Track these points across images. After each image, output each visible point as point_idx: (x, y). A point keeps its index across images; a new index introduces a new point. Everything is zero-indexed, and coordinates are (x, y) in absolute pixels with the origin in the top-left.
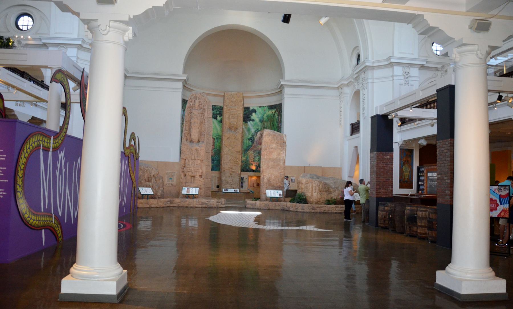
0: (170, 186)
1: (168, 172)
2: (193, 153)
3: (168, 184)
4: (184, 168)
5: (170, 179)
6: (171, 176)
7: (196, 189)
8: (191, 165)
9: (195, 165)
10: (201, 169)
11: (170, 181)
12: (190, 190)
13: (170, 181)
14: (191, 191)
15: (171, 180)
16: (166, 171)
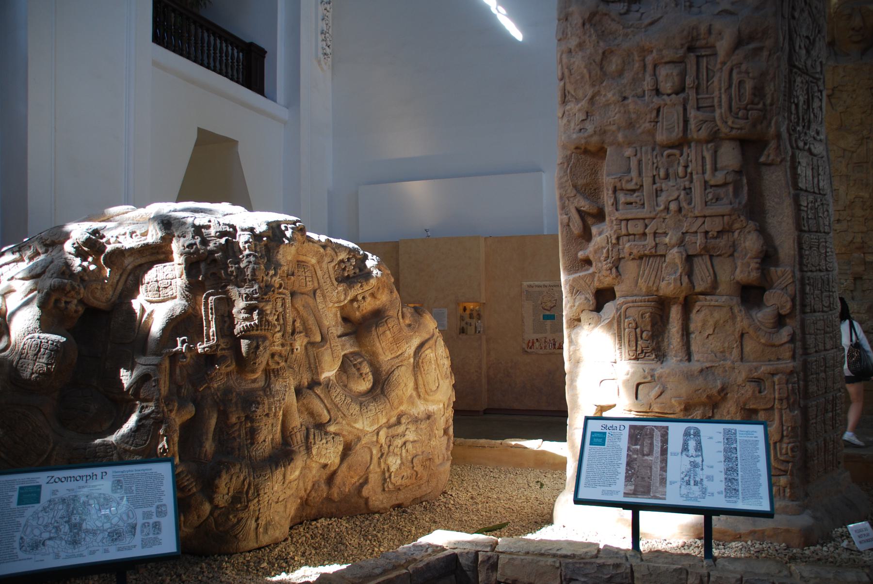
0: (550, 354)
1: (532, 283)
2: (667, 87)
3: (537, 344)
4: (594, 230)
5: (546, 317)
6: (549, 304)
7: (730, 439)
8: (658, 192)
9: (688, 191)
10: (751, 224)
11: (548, 327)
12: (664, 452)
13: (548, 327)
14: (677, 465)
15: (548, 322)
16: (525, 284)
